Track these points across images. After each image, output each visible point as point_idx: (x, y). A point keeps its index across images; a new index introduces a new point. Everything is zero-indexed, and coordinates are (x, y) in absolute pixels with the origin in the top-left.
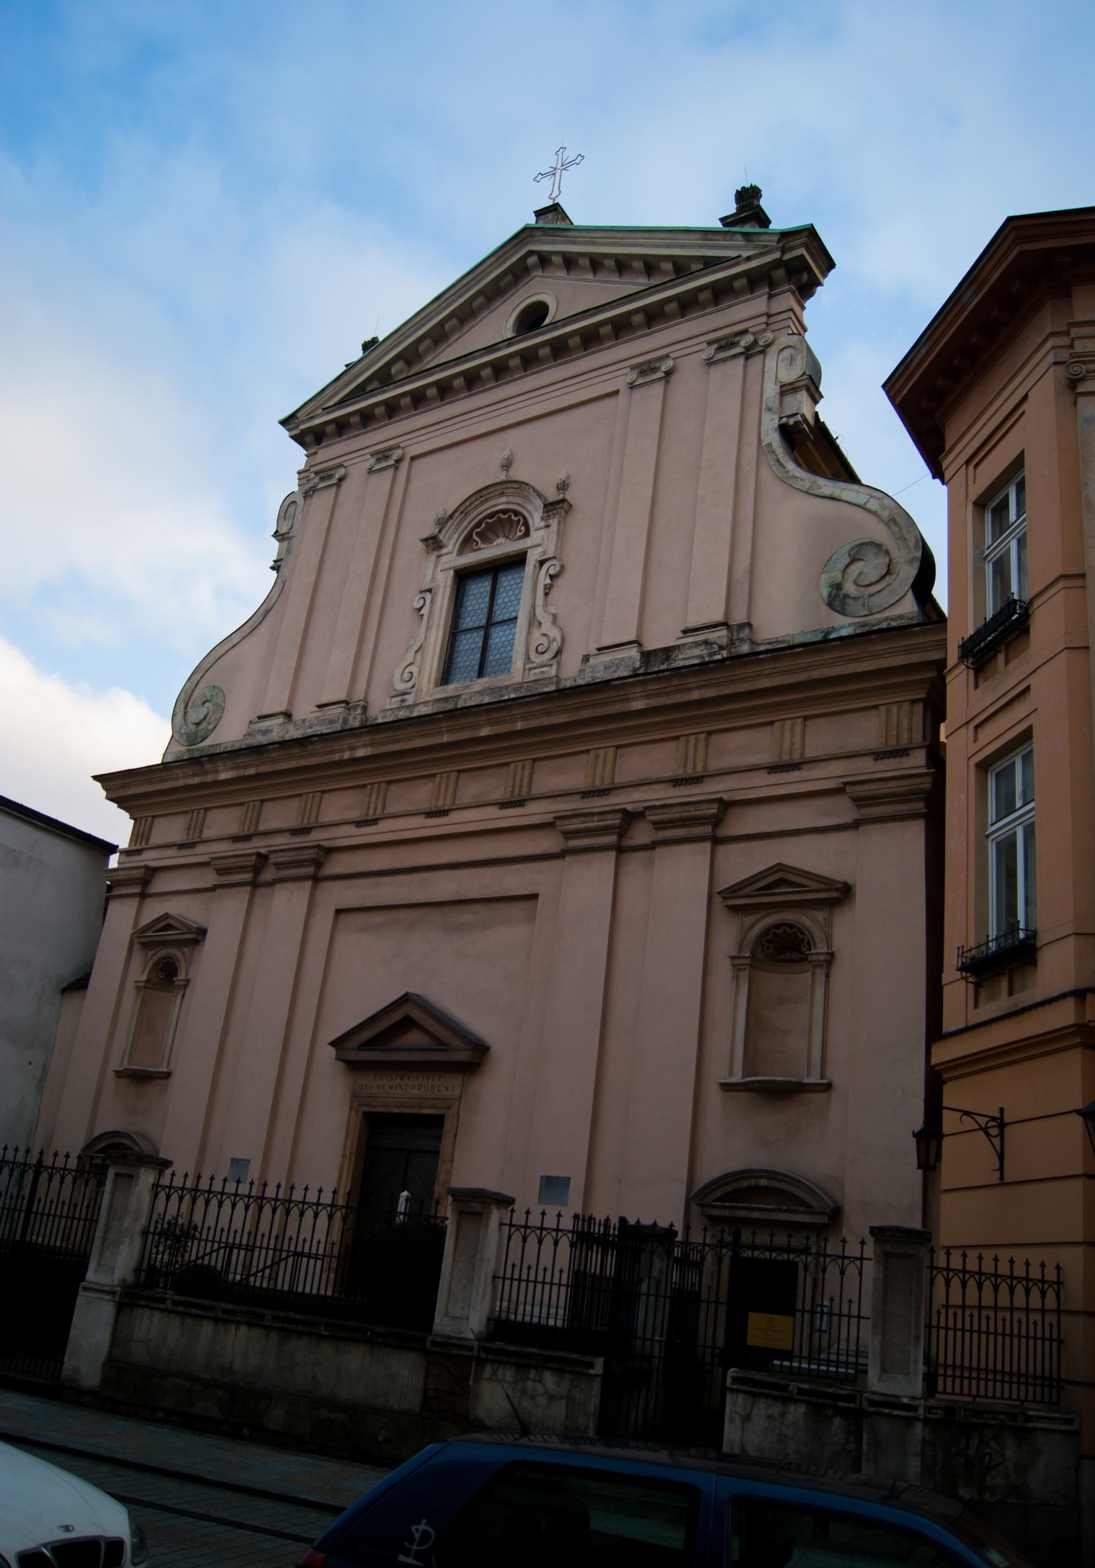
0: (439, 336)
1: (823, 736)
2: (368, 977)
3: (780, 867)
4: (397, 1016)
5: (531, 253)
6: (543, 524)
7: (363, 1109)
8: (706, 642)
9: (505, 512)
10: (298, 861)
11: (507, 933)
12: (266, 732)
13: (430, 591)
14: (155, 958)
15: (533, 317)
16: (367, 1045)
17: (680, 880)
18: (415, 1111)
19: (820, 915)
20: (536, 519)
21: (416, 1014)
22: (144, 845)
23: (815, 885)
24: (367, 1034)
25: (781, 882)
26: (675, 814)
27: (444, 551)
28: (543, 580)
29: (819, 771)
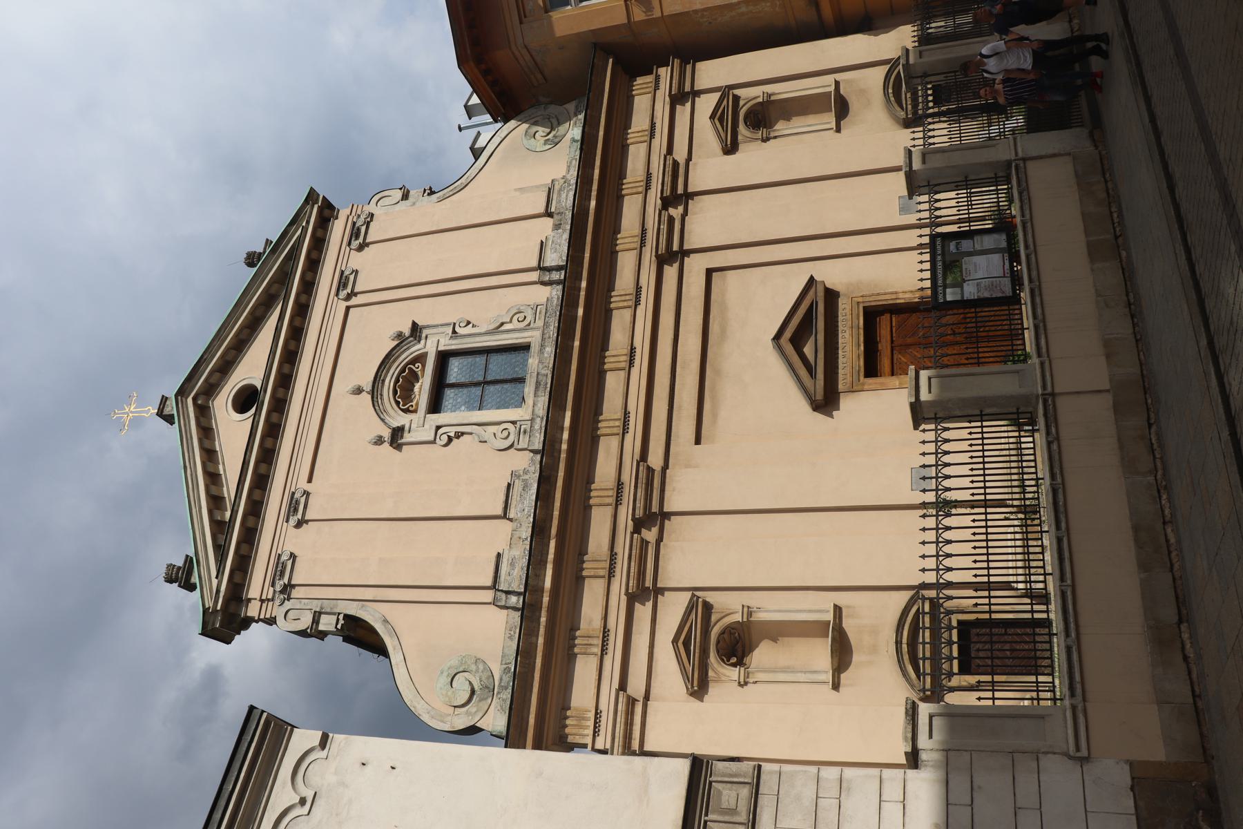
0: (213, 478)
1: (639, 122)
2: (755, 381)
3: (712, 117)
4: (789, 349)
5: (194, 399)
6: (423, 342)
7: (862, 378)
8: (560, 190)
9: (397, 381)
10: (647, 484)
11: (731, 288)
12: (512, 564)
13: (438, 428)
14: (716, 665)
15: (246, 400)
16: (811, 370)
17: (711, 167)
18: (862, 332)
19: (742, 103)
20: (416, 349)
21: (788, 334)
22: (592, 715)
23: (725, 102)
24: (803, 372)
25: (721, 120)
26: (668, 179)
27: (407, 428)
28: (469, 330)
29: (658, 113)
